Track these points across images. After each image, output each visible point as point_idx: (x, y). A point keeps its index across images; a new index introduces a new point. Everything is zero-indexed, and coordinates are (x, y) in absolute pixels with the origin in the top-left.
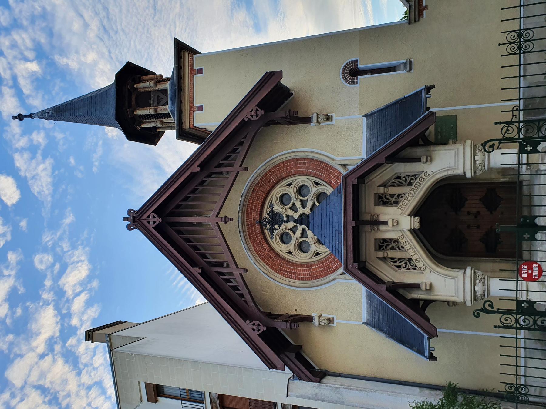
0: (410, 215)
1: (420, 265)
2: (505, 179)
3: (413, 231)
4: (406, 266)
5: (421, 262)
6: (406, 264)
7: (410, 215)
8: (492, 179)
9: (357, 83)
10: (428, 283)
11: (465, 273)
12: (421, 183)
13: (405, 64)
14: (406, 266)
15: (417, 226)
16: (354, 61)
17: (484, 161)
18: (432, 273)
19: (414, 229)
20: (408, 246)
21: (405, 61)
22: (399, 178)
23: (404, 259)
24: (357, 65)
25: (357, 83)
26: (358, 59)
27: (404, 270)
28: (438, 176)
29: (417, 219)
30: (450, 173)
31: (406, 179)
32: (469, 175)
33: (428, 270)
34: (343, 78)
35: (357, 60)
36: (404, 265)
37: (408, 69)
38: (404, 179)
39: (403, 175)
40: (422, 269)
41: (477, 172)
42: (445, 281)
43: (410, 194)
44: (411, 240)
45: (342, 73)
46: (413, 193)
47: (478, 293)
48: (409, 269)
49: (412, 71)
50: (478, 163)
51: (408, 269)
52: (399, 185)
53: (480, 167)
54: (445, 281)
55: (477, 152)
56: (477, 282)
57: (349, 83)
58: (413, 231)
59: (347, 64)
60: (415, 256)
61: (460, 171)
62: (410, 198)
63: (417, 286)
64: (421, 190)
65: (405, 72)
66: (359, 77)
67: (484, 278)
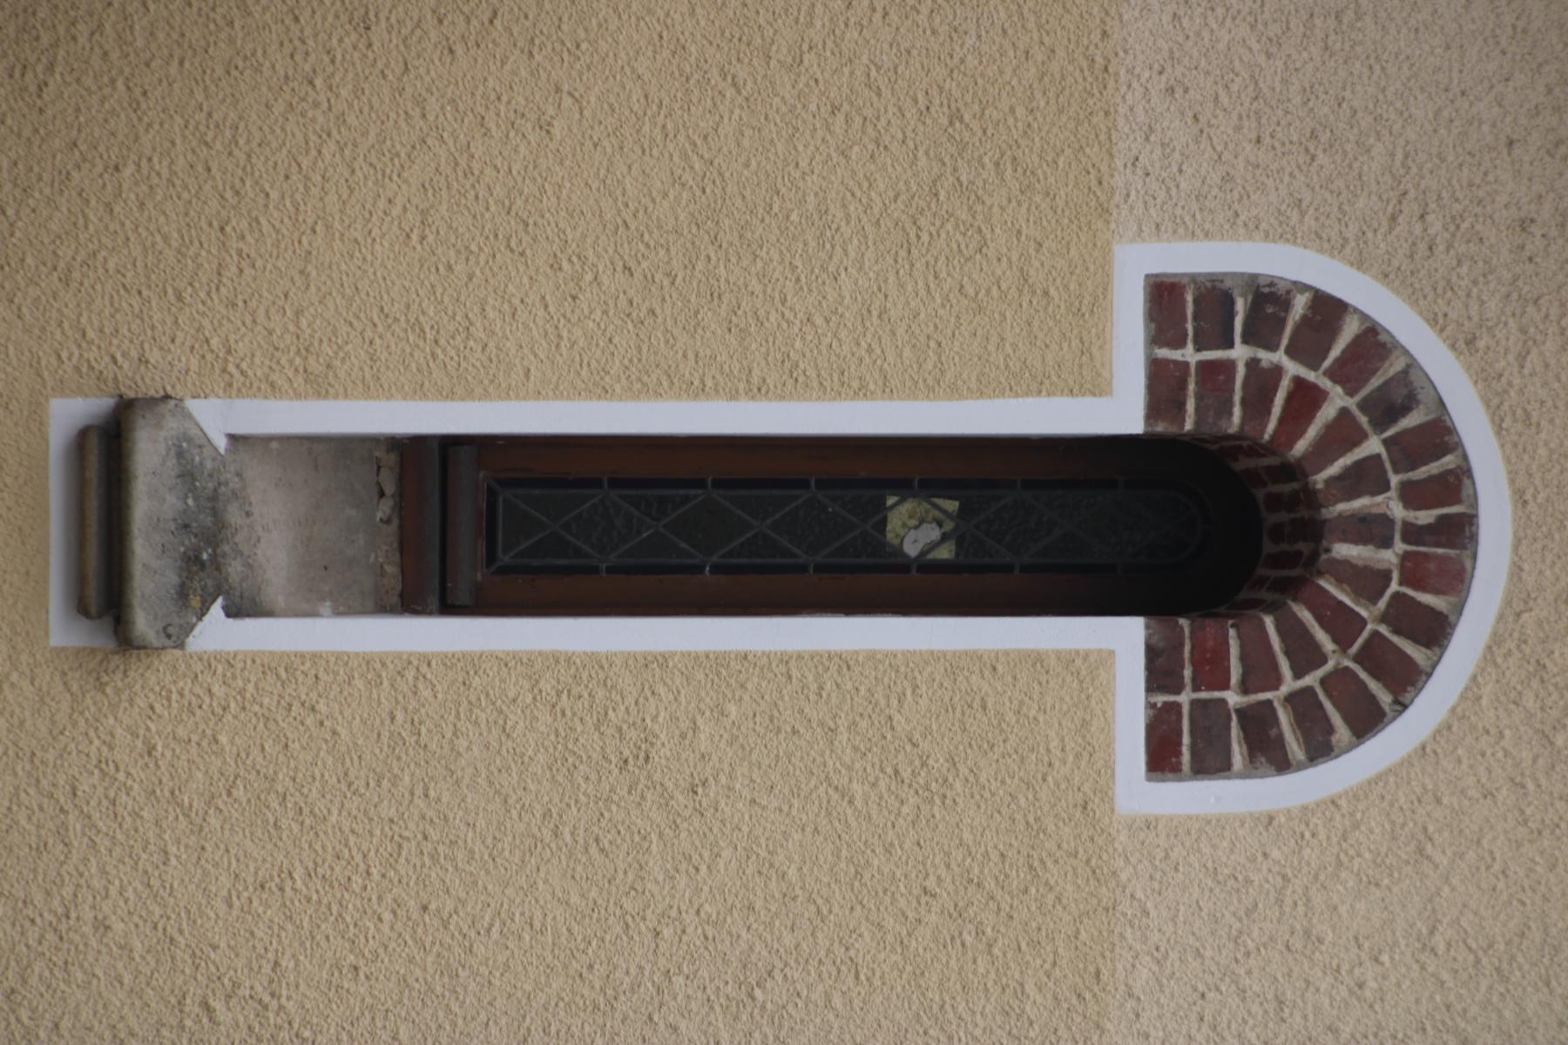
9: (1164, 295)
13: (211, 573)
16: (1211, 763)
21: (217, 632)
24: (1160, 673)
25: (1164, 295)
26: (1138, 793)
34: (1440, 436)
35: (1162, 759)
37: (149, 453)
45: (1459, 531)
49: (69, 412)
57: (1328, 310)
59: (1367, 721)
65: (217, 418)
66: (1121, 411)
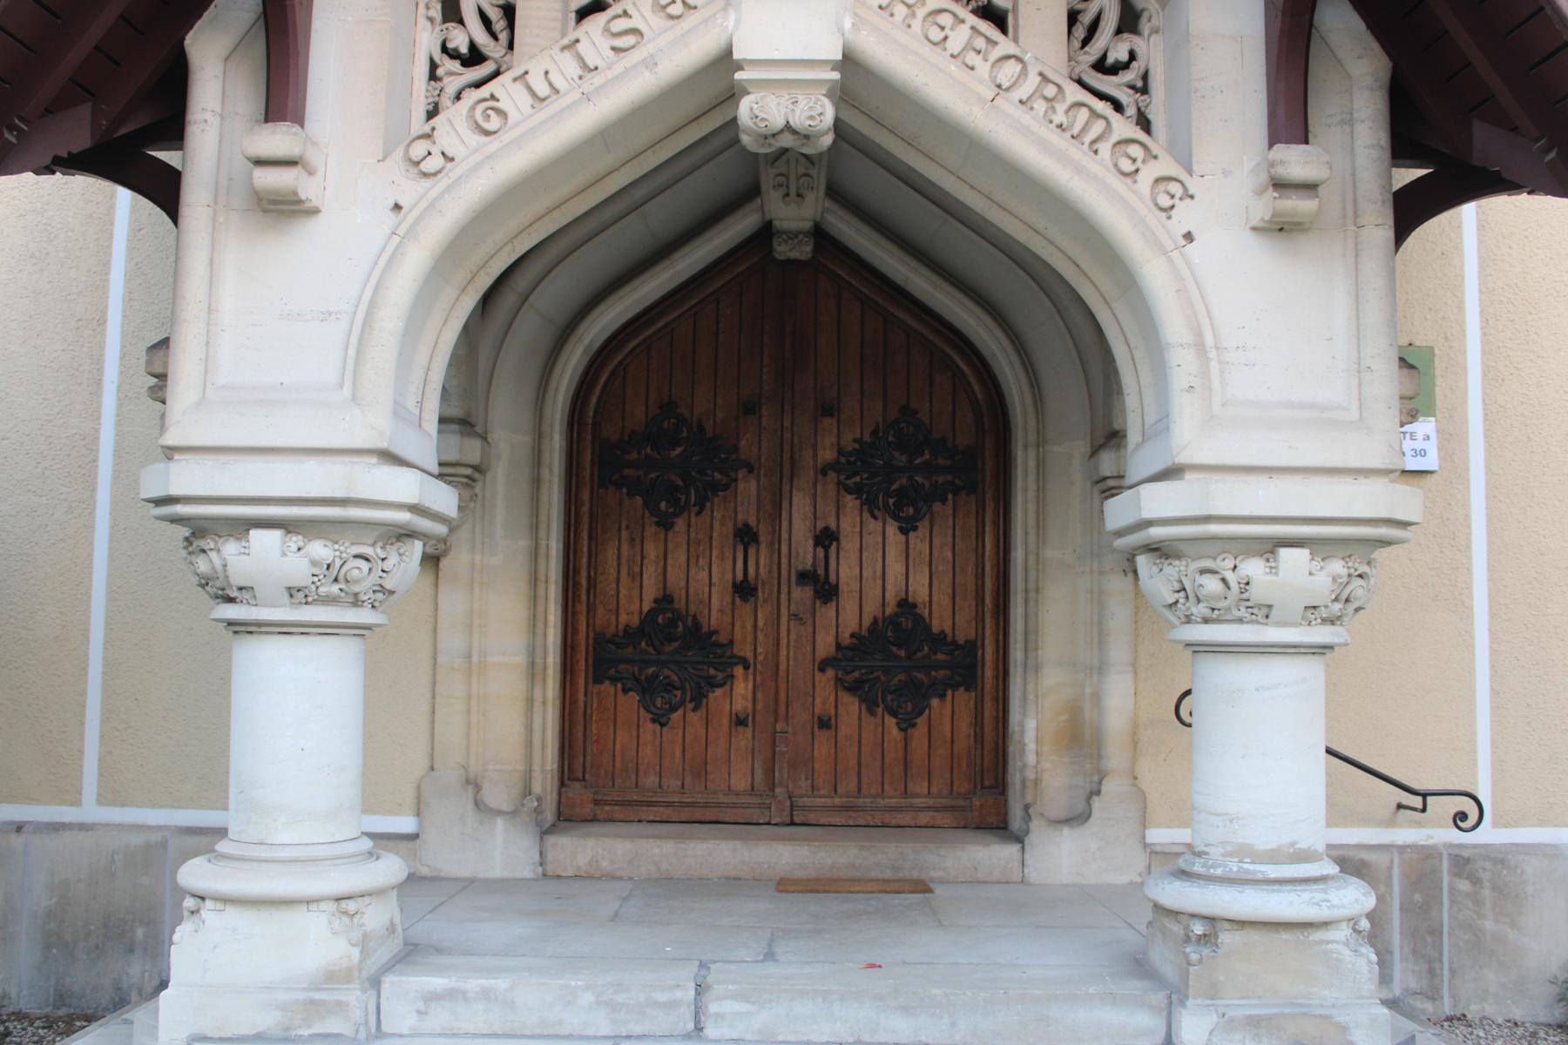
0: (850, 63)
1: (454, 129)
2: (1031, 746)
3: (721, 77)
4: (453, 54)
5: (475, 139)
6: (474, 57)
7: (850, 63)
8: (1033, 667)
10: (309, 189)
11: (390, 457)
12: (1105, 148)
14: (453, 54)
15: (763, 111)
17: (1265, 612)
18: (392, 217)
19: (733, 94)
20: (605, 44)
22: (1129, 22)
23: (511, 46)
27: (427, 40)
28: (1155, 275)
29: (814, 113)
30: (1182, 365)
31: (1114, 70)
32: (1156, 502)
33: (410, 191)
36: (460, 42)
38: (1119, 53)
39: (1151, 49)
40: (419, 149)
41: (1172, 570)
42: (326, 316)
43: (1012, 68)
44: (650, 63)
46: (1023, 92)
47: (231, 548)
48: (433, 76)
50: (1254, 568)
51: (433, 66)
52: (1073, 17)
53: (1211, 585)
54: (326, 316)
55: (1337, 567)
56: (320, 550)
58: (721, 77)
60: (525, 100)
61: (1189, 437)
62: (983, 68)
63: (281, 95)
64: (1045, 146)
67: (356, 602)
